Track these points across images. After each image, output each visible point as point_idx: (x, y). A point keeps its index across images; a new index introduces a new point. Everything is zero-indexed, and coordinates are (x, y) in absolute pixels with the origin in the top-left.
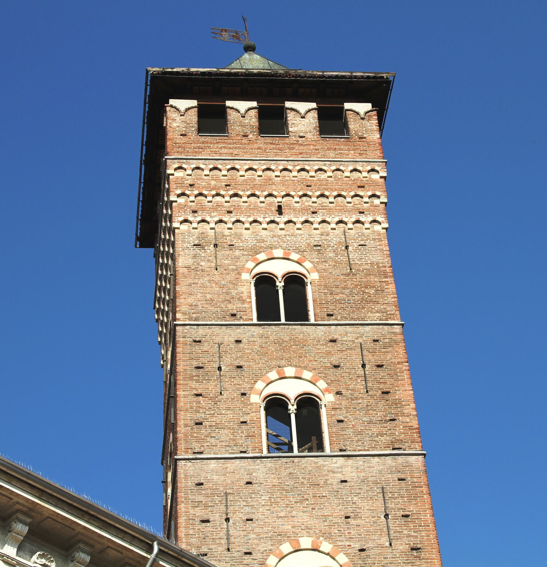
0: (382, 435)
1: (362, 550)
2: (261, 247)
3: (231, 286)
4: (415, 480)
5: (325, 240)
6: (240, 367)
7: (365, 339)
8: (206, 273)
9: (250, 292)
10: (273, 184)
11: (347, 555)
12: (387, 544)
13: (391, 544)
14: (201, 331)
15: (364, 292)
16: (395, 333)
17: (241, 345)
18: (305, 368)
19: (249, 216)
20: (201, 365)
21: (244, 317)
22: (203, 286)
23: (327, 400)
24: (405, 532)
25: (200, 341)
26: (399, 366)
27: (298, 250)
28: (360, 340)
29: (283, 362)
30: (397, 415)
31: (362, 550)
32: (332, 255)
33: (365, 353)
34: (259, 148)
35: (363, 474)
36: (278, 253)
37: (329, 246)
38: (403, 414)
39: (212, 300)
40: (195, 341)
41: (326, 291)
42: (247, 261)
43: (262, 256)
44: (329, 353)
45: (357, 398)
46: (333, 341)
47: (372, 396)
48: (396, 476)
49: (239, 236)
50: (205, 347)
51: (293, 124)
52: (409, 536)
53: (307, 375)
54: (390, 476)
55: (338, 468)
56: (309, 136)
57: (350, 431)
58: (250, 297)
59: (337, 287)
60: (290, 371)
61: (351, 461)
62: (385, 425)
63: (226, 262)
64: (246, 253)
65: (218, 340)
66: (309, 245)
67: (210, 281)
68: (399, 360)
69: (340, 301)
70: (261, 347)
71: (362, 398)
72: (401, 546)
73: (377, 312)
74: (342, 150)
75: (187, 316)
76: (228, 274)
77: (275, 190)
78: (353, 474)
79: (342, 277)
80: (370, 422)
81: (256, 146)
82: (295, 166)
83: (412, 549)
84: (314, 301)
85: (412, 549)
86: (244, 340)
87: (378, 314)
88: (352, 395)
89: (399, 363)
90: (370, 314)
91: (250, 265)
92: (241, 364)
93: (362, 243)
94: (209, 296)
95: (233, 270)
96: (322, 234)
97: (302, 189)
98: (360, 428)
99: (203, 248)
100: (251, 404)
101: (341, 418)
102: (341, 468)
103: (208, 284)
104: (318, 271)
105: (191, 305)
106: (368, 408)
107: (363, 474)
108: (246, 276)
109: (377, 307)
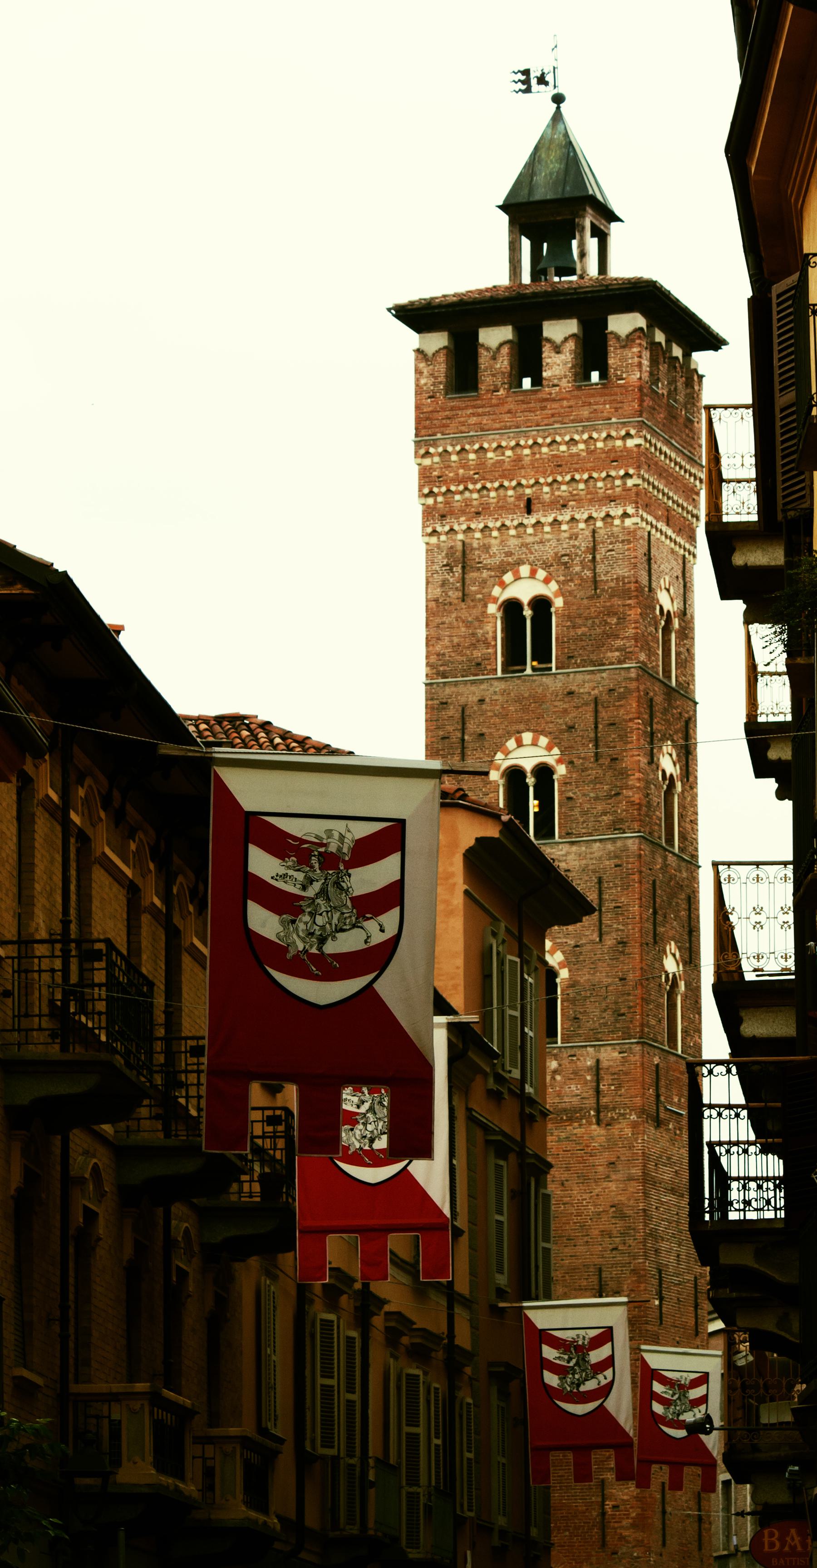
0: (605, 813)
1: (577, 946)
2: (509, 564)
3: (476, 624)
4: (630, 866)
5: (574, 546)
6: (482, 735)
7: (601, 689)
8: (453, 607)
9: (495, 632)
10: (523, 467)
11: (563, 952)
12: (598, 939)
13: (600, 940)
14: (448, 690)
15: (606, 623)
16: (631, 679)
17: (484, 706)
18: (543, 733)
19: (497, 519)
20: (447, 735)
21: (489, 667)
22: (451, 627)
23: (561, 770)
24: (615, 926)
25: (446, 703)
26: (630, 724)
27: (546, 566)
28: (596, 691)
29: (522, 727)
30: (621, 788)
31: (577, 946)
32: (578, 569)
33: (600, 708)
34: (509, 412)
35: (584, 862)
36: (525, 570)
37: (576, 555)
38: (627, 787)
39: (459, 645)
40: (442, 703)
41: (569, 623)
42: (493, 586)
43: (508, 577)
44: (565, 711)
45: (586, 769)
46: (571, 693)
47: (601, 765)
48: (612, 862)
49: (486, 548)
50: (451, 712)
51: (547, 364)
52: (618, 930)
53: (543, 741)
54: (608, 863)
55: (563, 856)
56: (564, 383)
57: (577, 812)
58: (495, 638)
59: (580, 616)
60: (527, 737)
61: (574, 848)
62: (609, 801)
63: (473, 588)
64: (493, 573)
65: (462, 700)
66: (556, 554)
67: (457, 619)
68: (631, 716)
69: (580, 638)
70: (503, 708)
71: (592, 769)
72: (609, 941)
73: (617, 650)
74: (597, 404)
75: (434, 671)
76: (474, 607)
77: (524, 477)
78: (576, 863)
79: (585, 602)
80: (597, 798)
81: (506, 407)
82: (544, 438)
83: (619, 943)
84: (557, 639)
85: (619, 943)
86: (487, 700)
87: (617, 654)
88: (582, 764)
89: (631, 720)
90: (609, 654)
91: (496, 591)
92: (484, 730)
93: (611, 547)
94: (456, 640)
95: (480, 600)
96: (570, 538)
97: (552, 473)
98: (586, 806)
99: (451, 570)
100: (490, 782)
101: (571, 794)
102: (566, 855)
103: (455, 623)
104: (563, 595)
105: (438, 655)
106: (597, 781)
107: (584, 862)
108: (492, 609)
109: (619, 643)
